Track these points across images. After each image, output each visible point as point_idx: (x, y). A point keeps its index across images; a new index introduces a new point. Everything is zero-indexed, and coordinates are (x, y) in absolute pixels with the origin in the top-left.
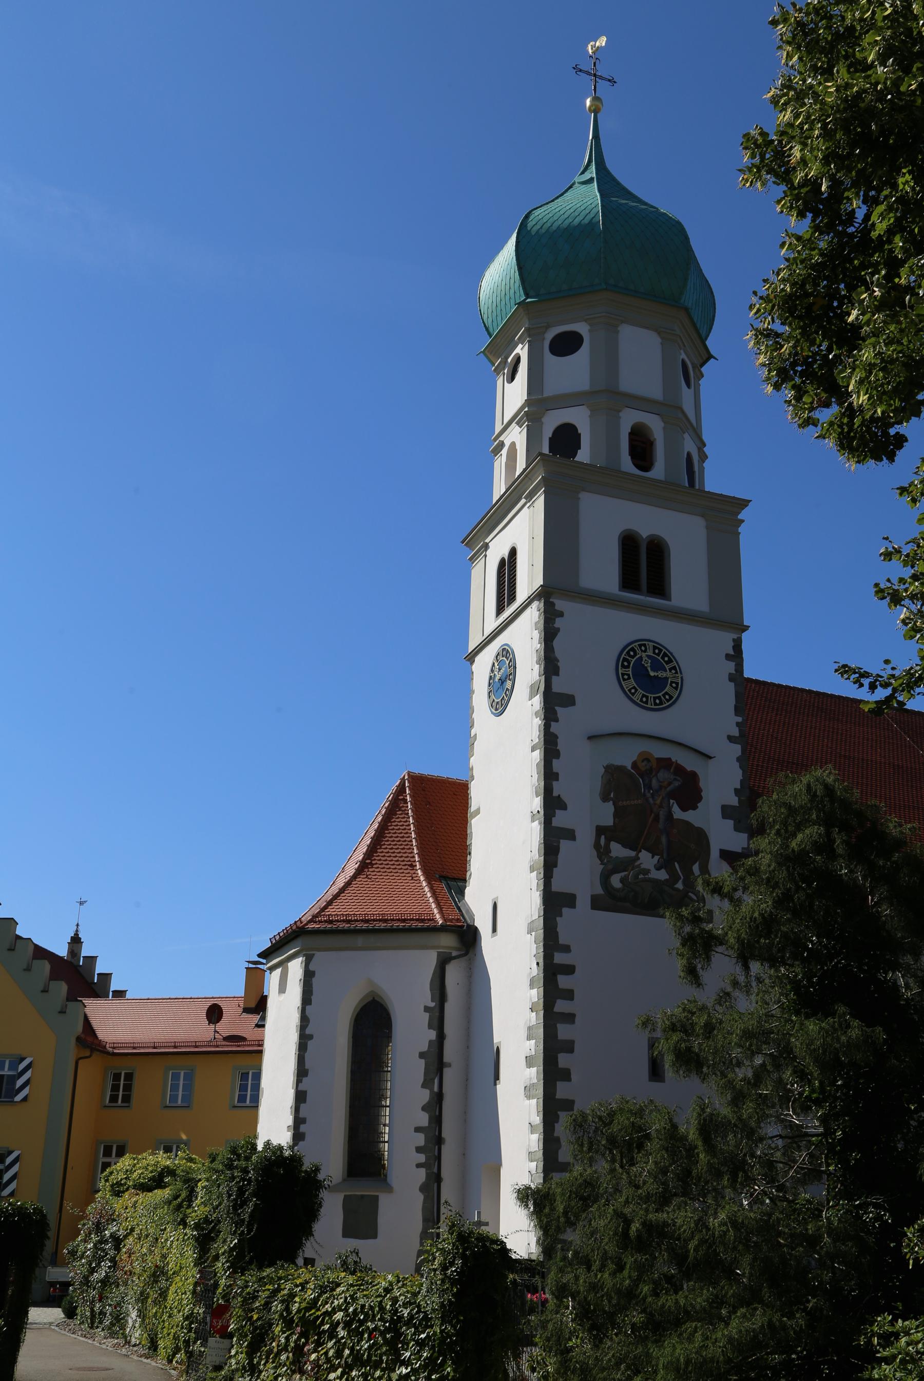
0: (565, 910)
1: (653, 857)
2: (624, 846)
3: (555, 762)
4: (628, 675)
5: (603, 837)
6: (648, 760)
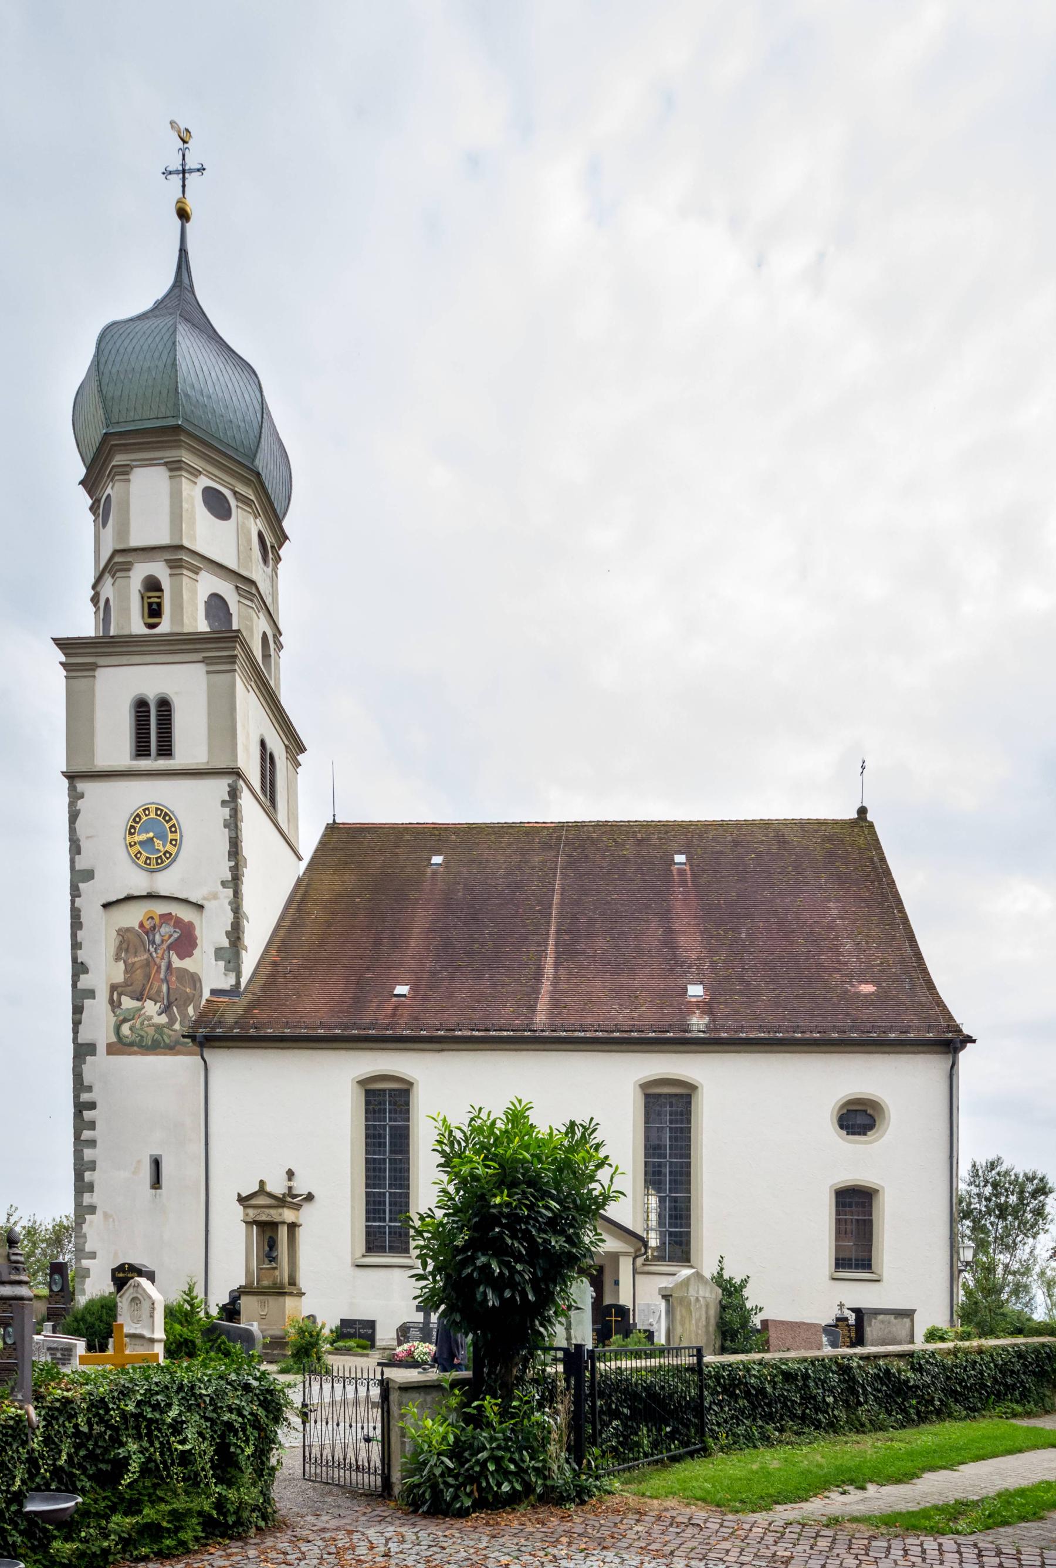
0: (88, 1058)
2: (132, 998)
3: (79, 933)
5: (115, 993)
6: (152, 918)
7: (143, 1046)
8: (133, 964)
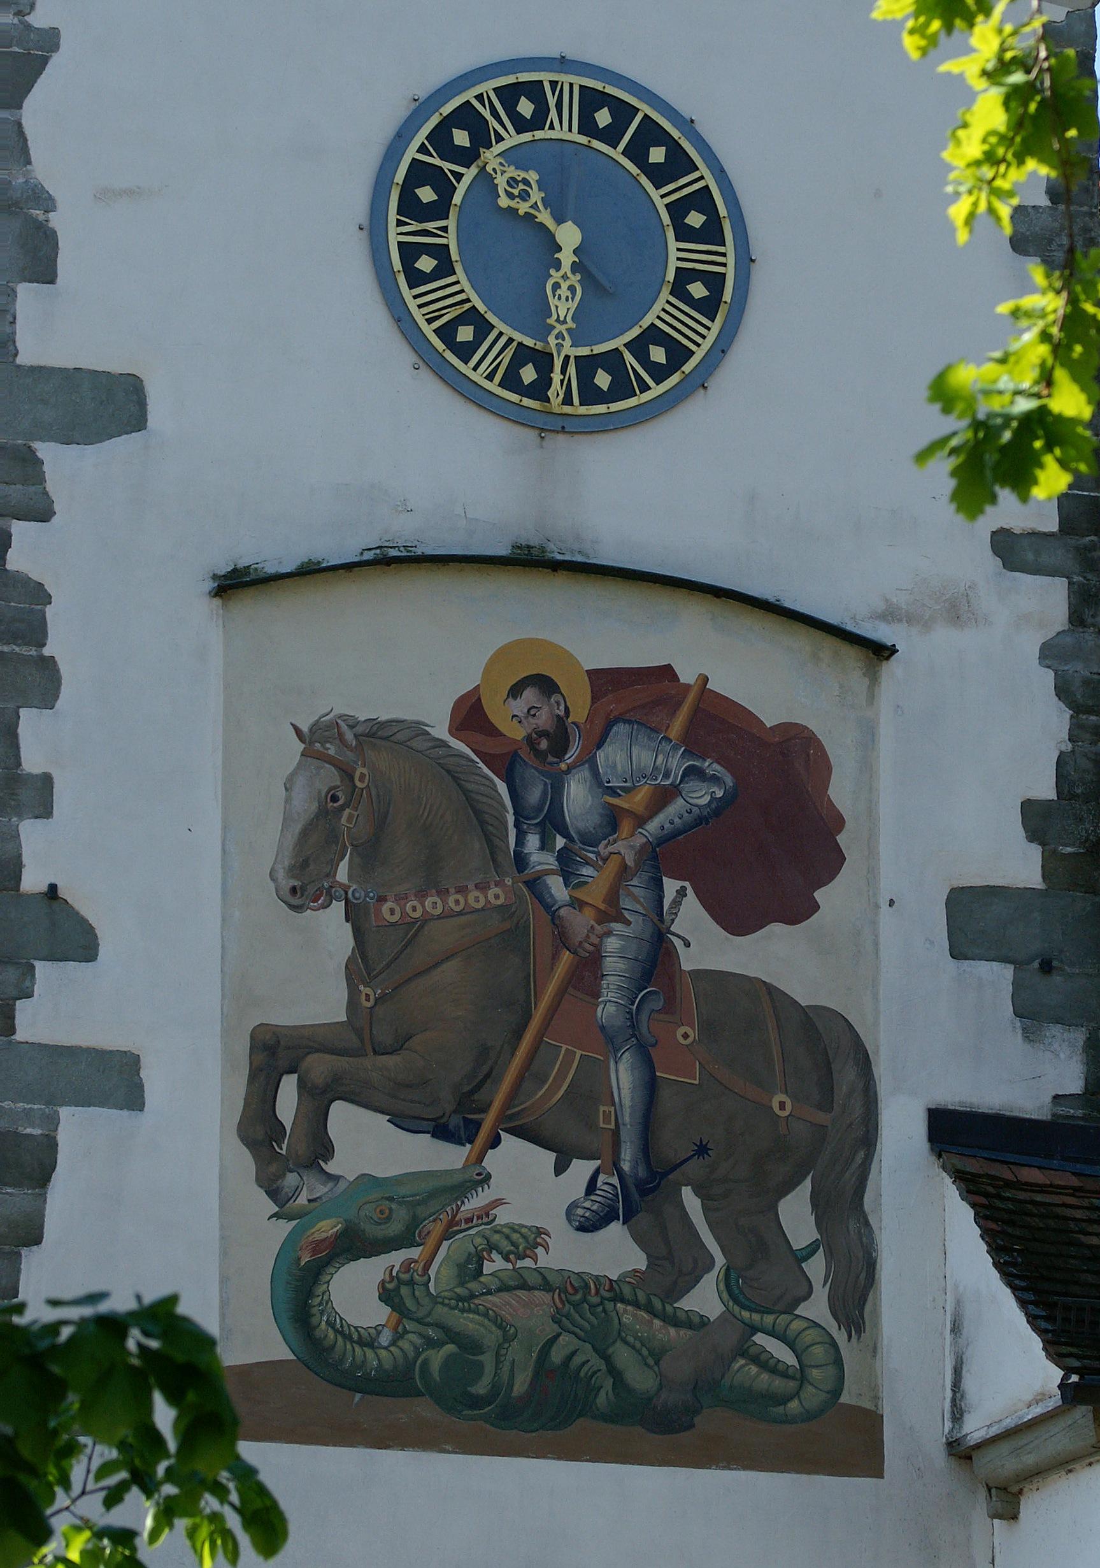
1: (560, 1168)
4: (441, 253)
6: (546, 685)
7: (476, 1402)
8: (413, 930)
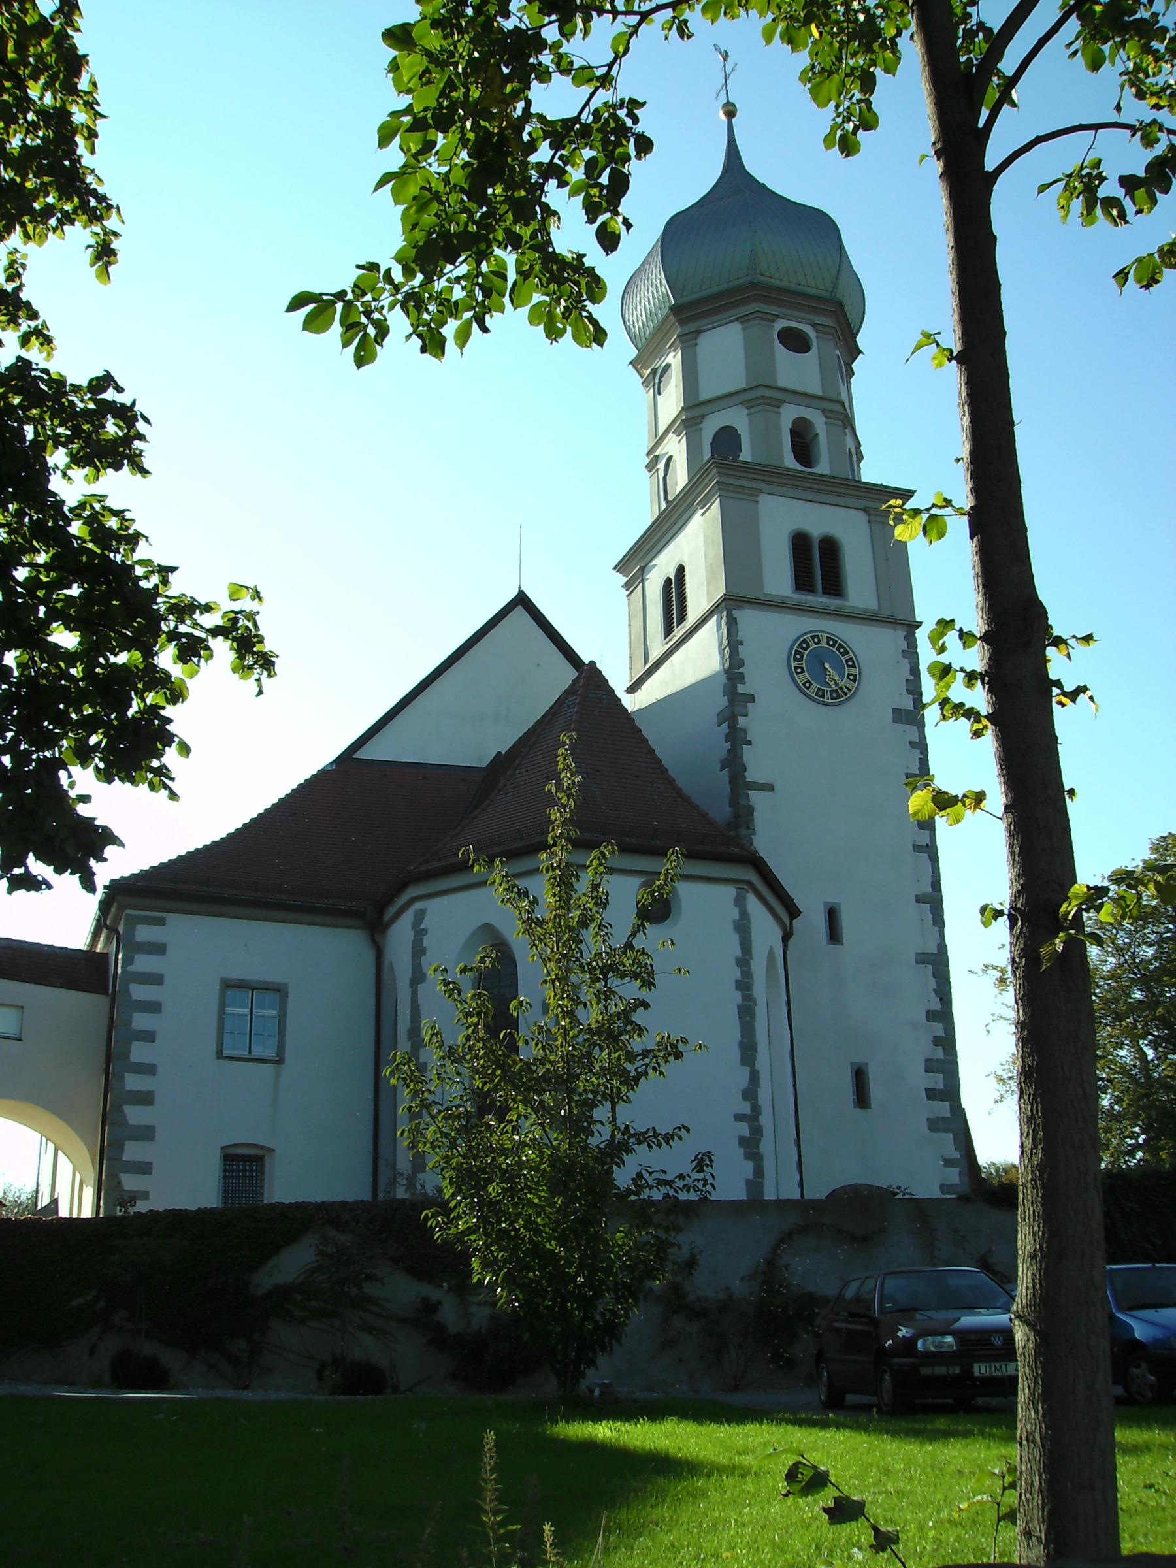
4: (802, 668)
